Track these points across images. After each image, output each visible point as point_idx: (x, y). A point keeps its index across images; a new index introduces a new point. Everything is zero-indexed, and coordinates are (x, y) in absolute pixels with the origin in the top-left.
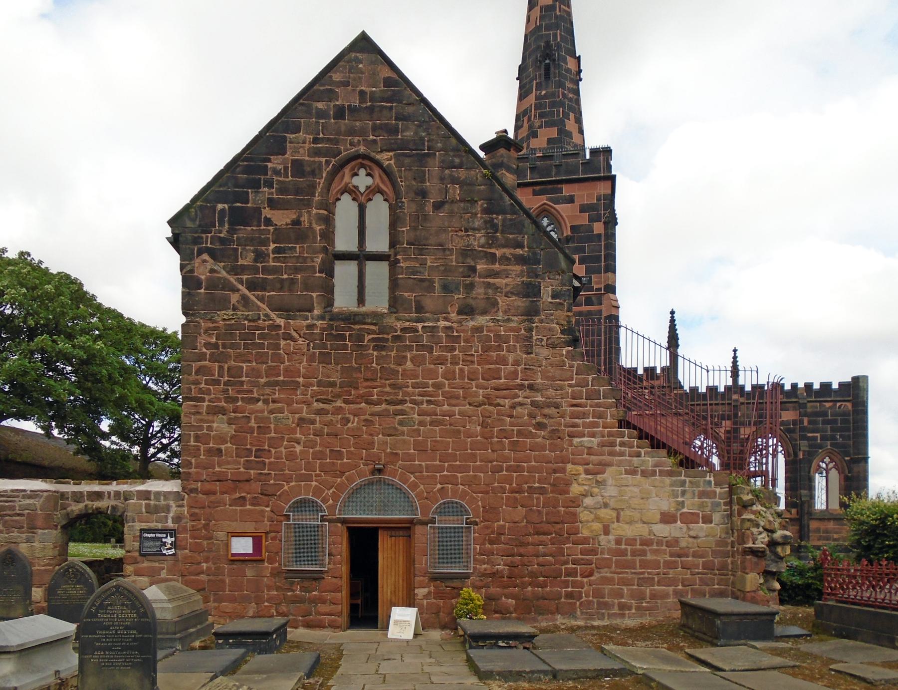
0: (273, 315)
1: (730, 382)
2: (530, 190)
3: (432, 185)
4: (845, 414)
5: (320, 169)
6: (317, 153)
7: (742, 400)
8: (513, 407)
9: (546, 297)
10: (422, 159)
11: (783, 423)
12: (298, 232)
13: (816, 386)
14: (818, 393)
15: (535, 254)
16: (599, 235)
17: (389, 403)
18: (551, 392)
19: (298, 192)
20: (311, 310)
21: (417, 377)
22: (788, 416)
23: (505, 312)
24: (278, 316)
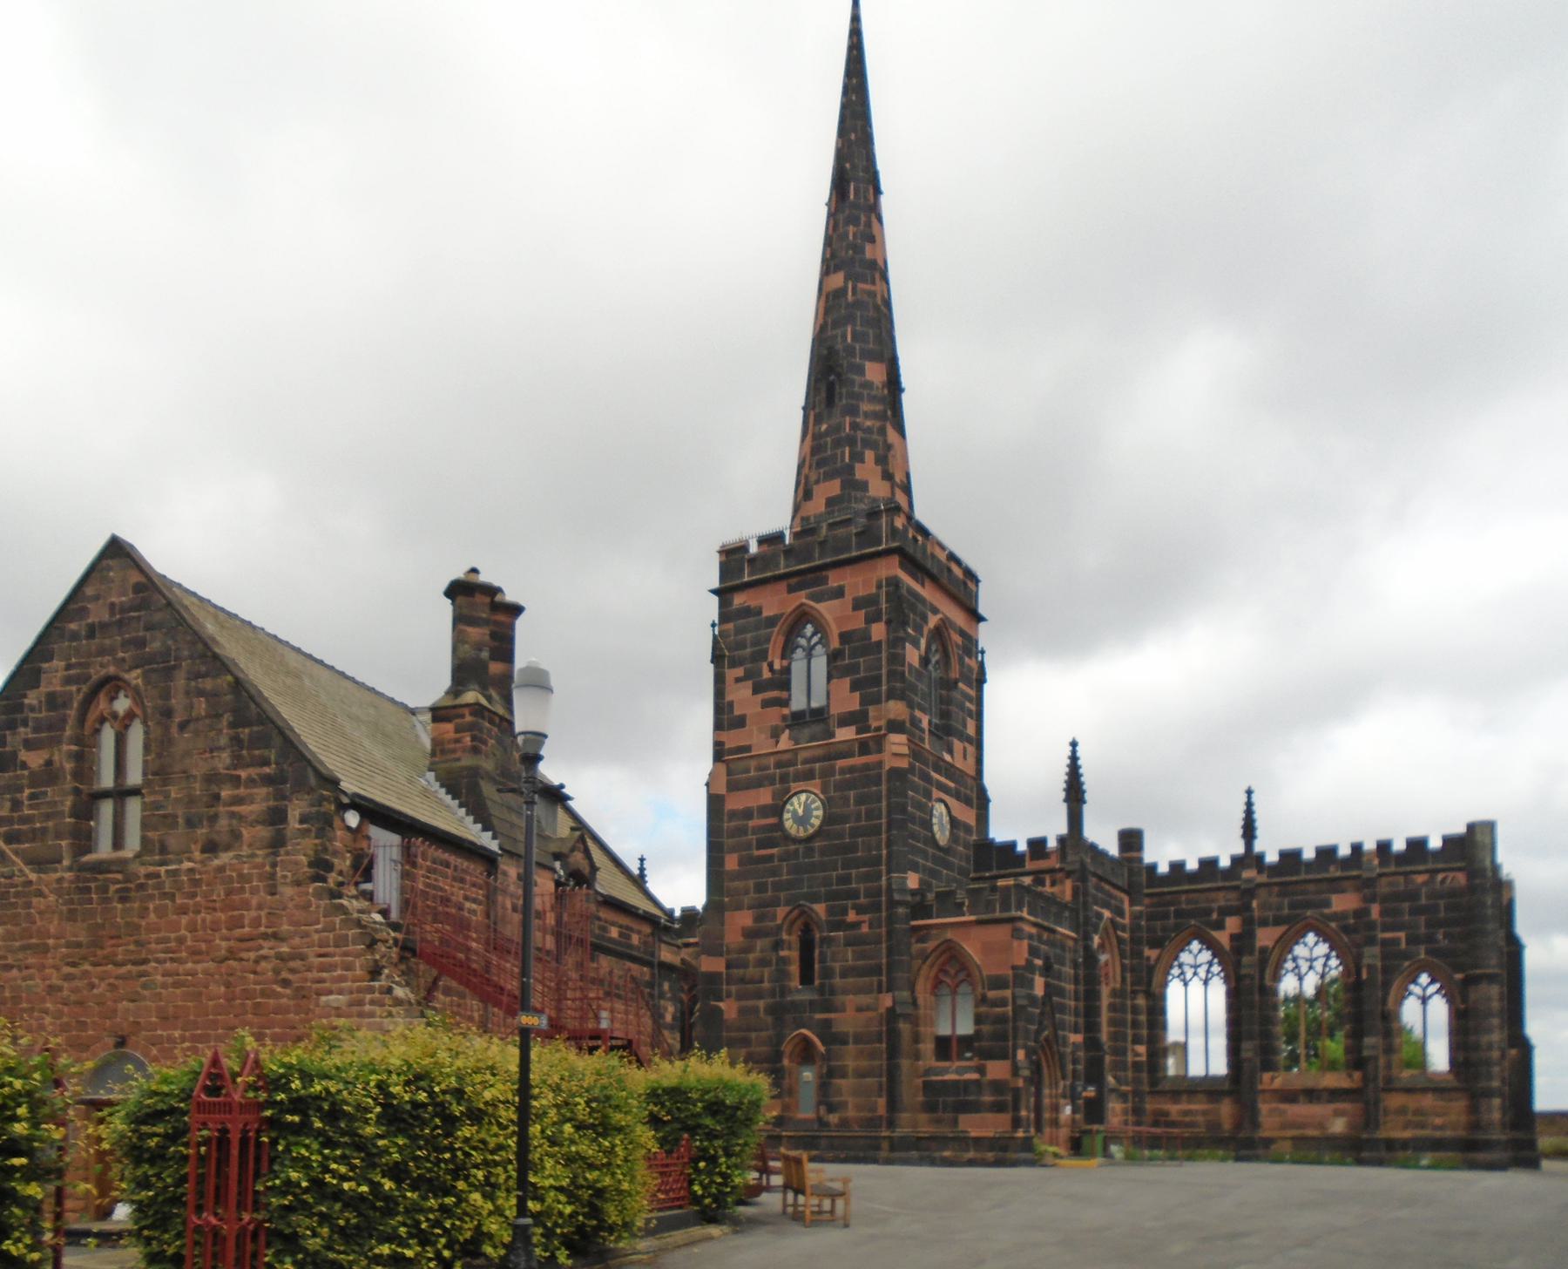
0: (27, 870)
1: (1239, 848)
2: (783, 585)
3: (178, 702)
4: (1453, 893)
5: (71, 699)
6: (68, 681)
7: (1263, 878)
8: (257, 962)
9: (294, 823)
10: (168, 673)
11: (1336, 917)
12: (49, 774)
14: (1401, 858)
15: (282, 770)
16: (879, 643)
17: (134, 963)
18: (297, 941)
19: (50, 728)
20: (60, 862)
21: (159, 930)
22: (1343, 902)
23: (250, 845)
24: (33, 871)
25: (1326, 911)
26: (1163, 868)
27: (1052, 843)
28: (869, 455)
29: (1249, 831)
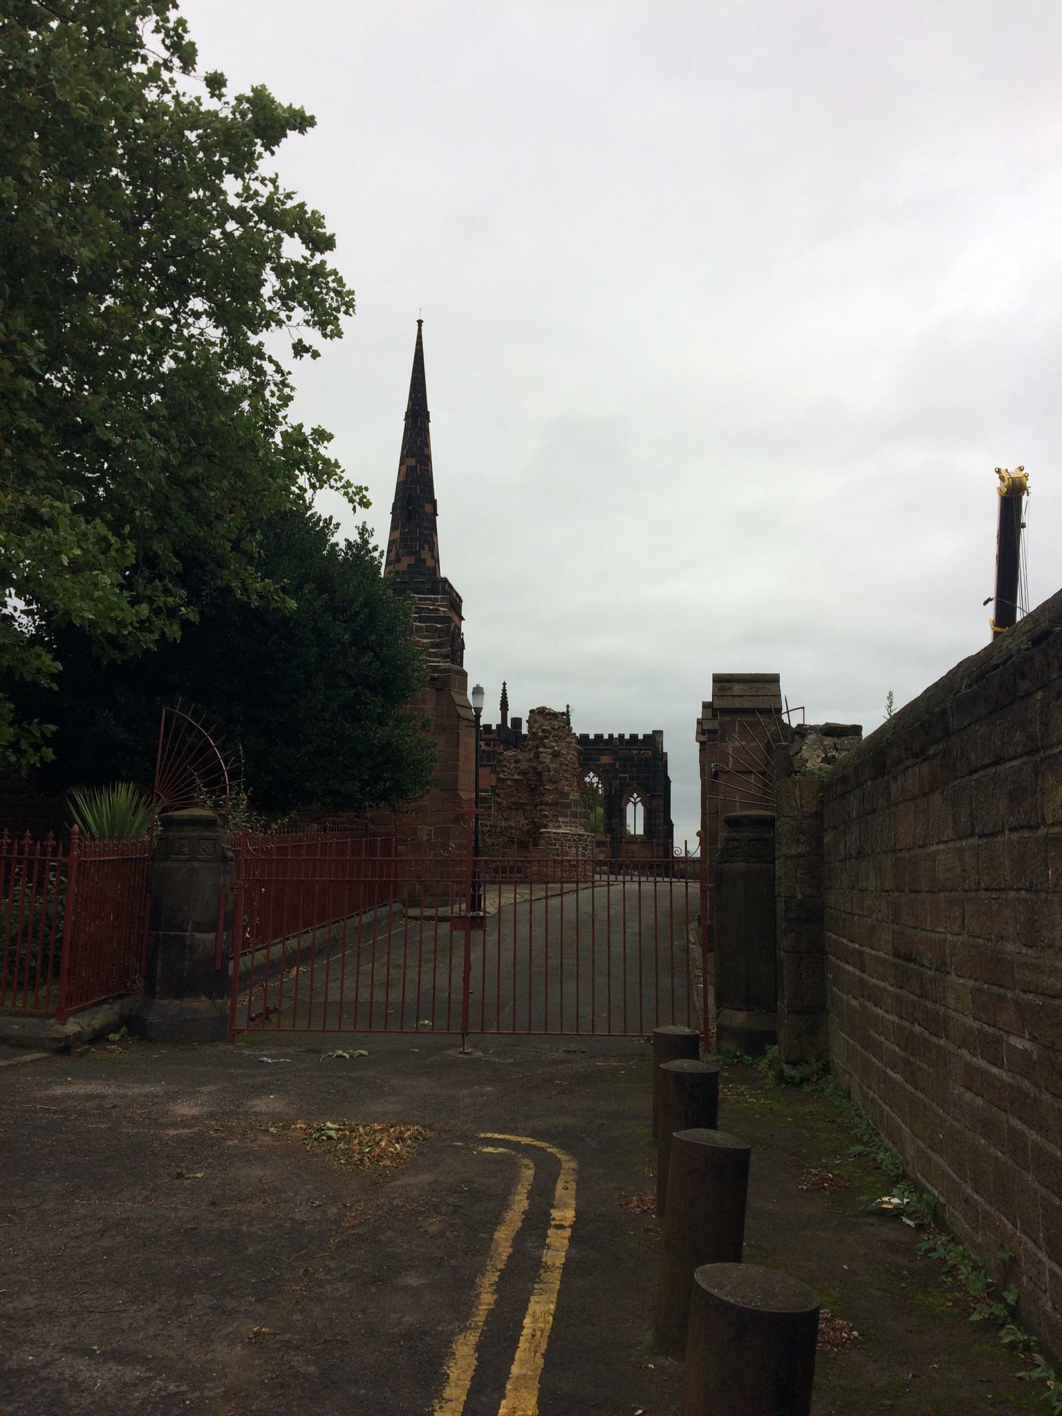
13: (627, 737)
22: (605, 760)
27: (494, 727)
28: (426, 547)
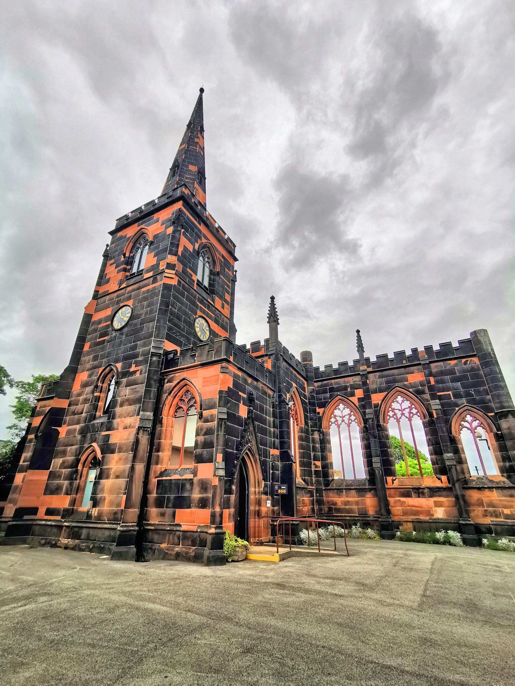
1: (357, 357)
7: (370, 369)
25: (405, 383)
26: (322, 369)
27: (262, 343)
29: (360, 348)
